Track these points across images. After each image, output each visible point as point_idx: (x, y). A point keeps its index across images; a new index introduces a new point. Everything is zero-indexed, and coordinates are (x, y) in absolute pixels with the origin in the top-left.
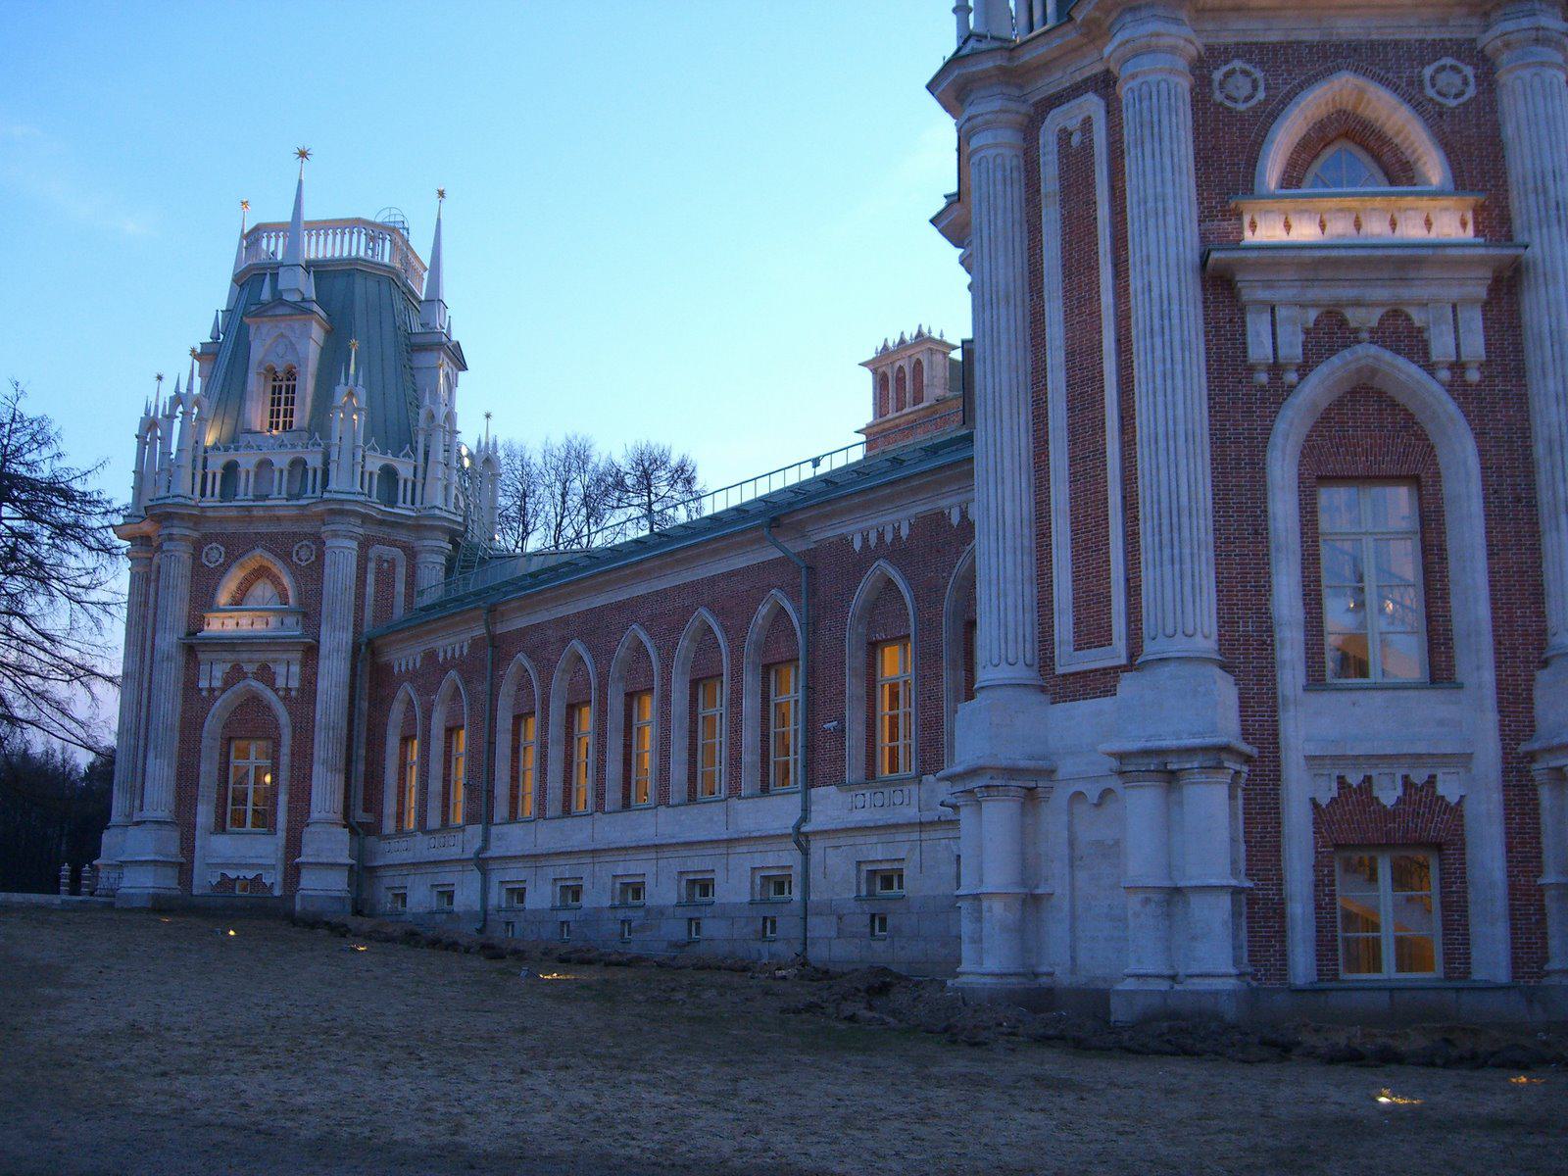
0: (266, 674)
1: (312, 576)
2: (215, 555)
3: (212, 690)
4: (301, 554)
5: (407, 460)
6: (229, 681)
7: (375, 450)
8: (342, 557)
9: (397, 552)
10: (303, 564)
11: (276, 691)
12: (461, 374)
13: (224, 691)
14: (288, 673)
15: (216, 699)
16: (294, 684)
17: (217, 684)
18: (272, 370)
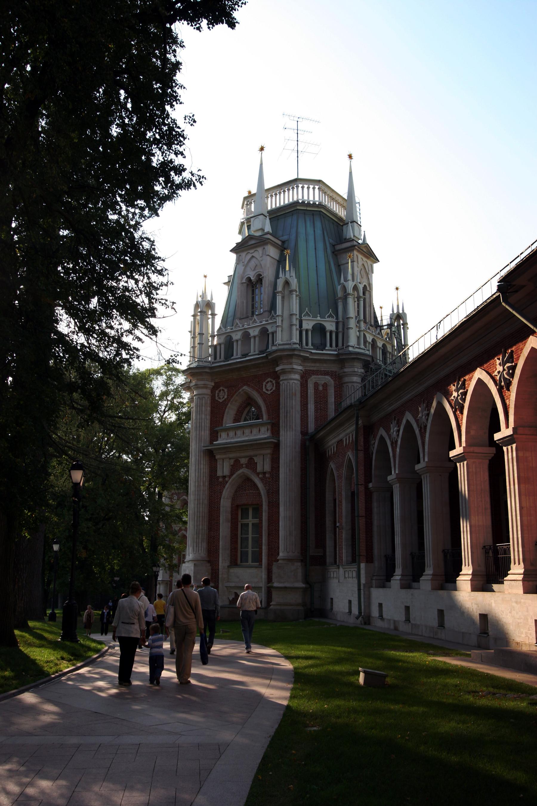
0: (252, 464)
3: (224, 477)
4: (270, 388)
5: (330, 319)
6: (233, 472)
9: (328, 379)
10: (269, 393)
11: (258, 474)
12: (375, 265)
13: (230, 477)
14: (264, 465)
15: (227, 482)
17: (227, 472)
18: (249, 279)
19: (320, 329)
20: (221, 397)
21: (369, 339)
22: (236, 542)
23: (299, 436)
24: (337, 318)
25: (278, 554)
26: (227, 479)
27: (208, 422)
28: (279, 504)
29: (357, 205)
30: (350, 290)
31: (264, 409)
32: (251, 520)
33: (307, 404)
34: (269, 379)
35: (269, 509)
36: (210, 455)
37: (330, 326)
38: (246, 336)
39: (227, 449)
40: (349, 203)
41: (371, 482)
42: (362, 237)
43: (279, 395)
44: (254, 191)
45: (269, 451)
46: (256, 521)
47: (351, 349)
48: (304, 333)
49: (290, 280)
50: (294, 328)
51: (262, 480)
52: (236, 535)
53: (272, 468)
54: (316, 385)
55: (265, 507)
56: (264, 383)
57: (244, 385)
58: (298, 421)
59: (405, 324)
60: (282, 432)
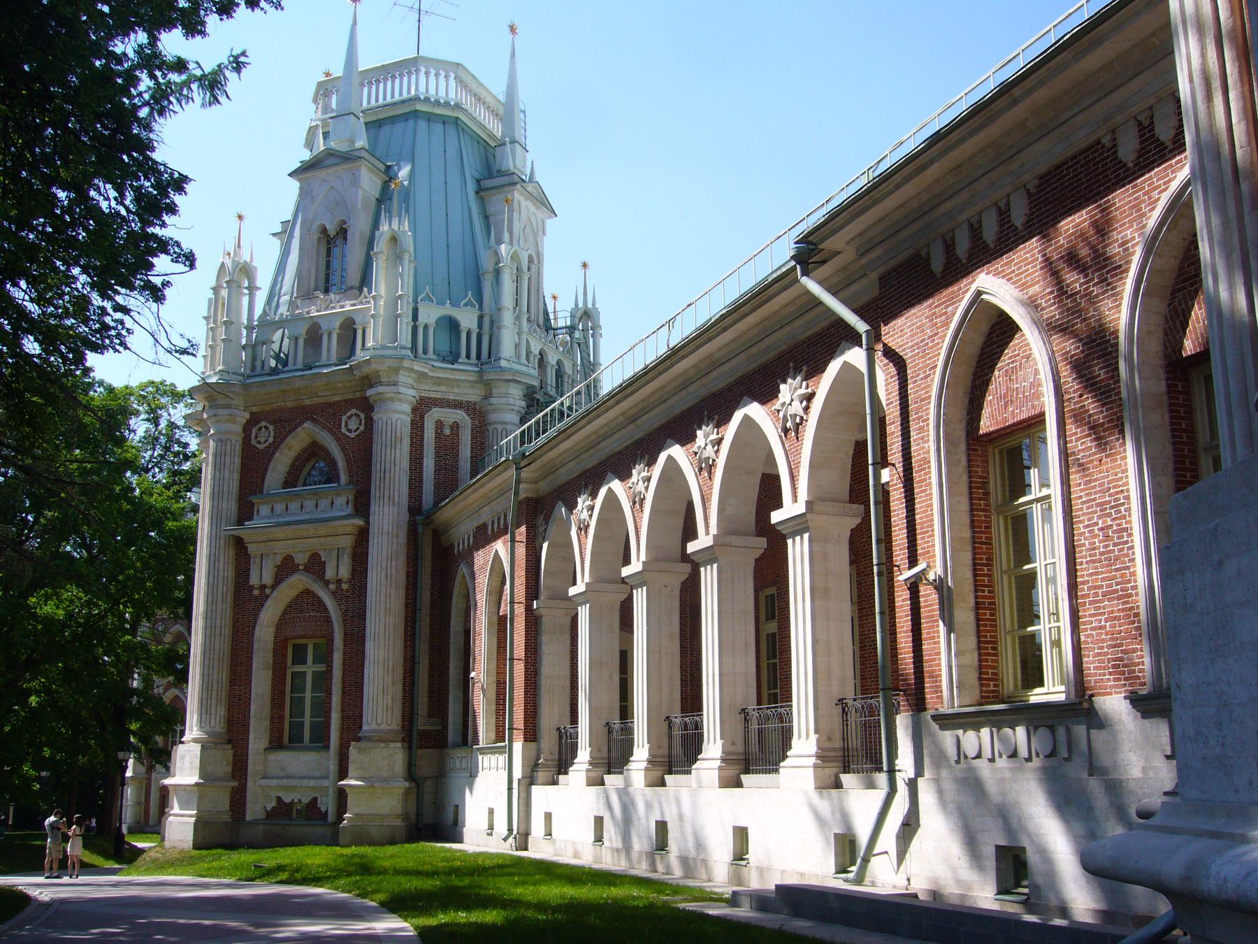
0: (316, 566)
1: (362, 454)
2: (264, 437)
3: (263, 587)
9: (460, 416)
10: (352, 435)
11: (327, 583)
12: (550, 223)
13: (273, 587)
16: (345, 572)
17: (268, 579)
19: (452, 326)
20: (263, 440)
21: (535, 350)
22: (282, 706)
23: (405, 516)
24: (481, 309)
26: (268, 591)
27: (236, 484)
32: (310, 668)
33: (422, 458)
34: (353, 411)
35: (345, 645)
37: (468, 319)
40: (508, 111)
41: (537, 598)
43: (371, 439)
44: (338, 71)
46: (321, 668)
47: (503, 363)
48: (421, 331)
51: (334, 593)
53: (354, 571)
54: (439, 425)
56: (344, 418)
57: (307, 419)
59: (596, 327)
60: (375, 508)
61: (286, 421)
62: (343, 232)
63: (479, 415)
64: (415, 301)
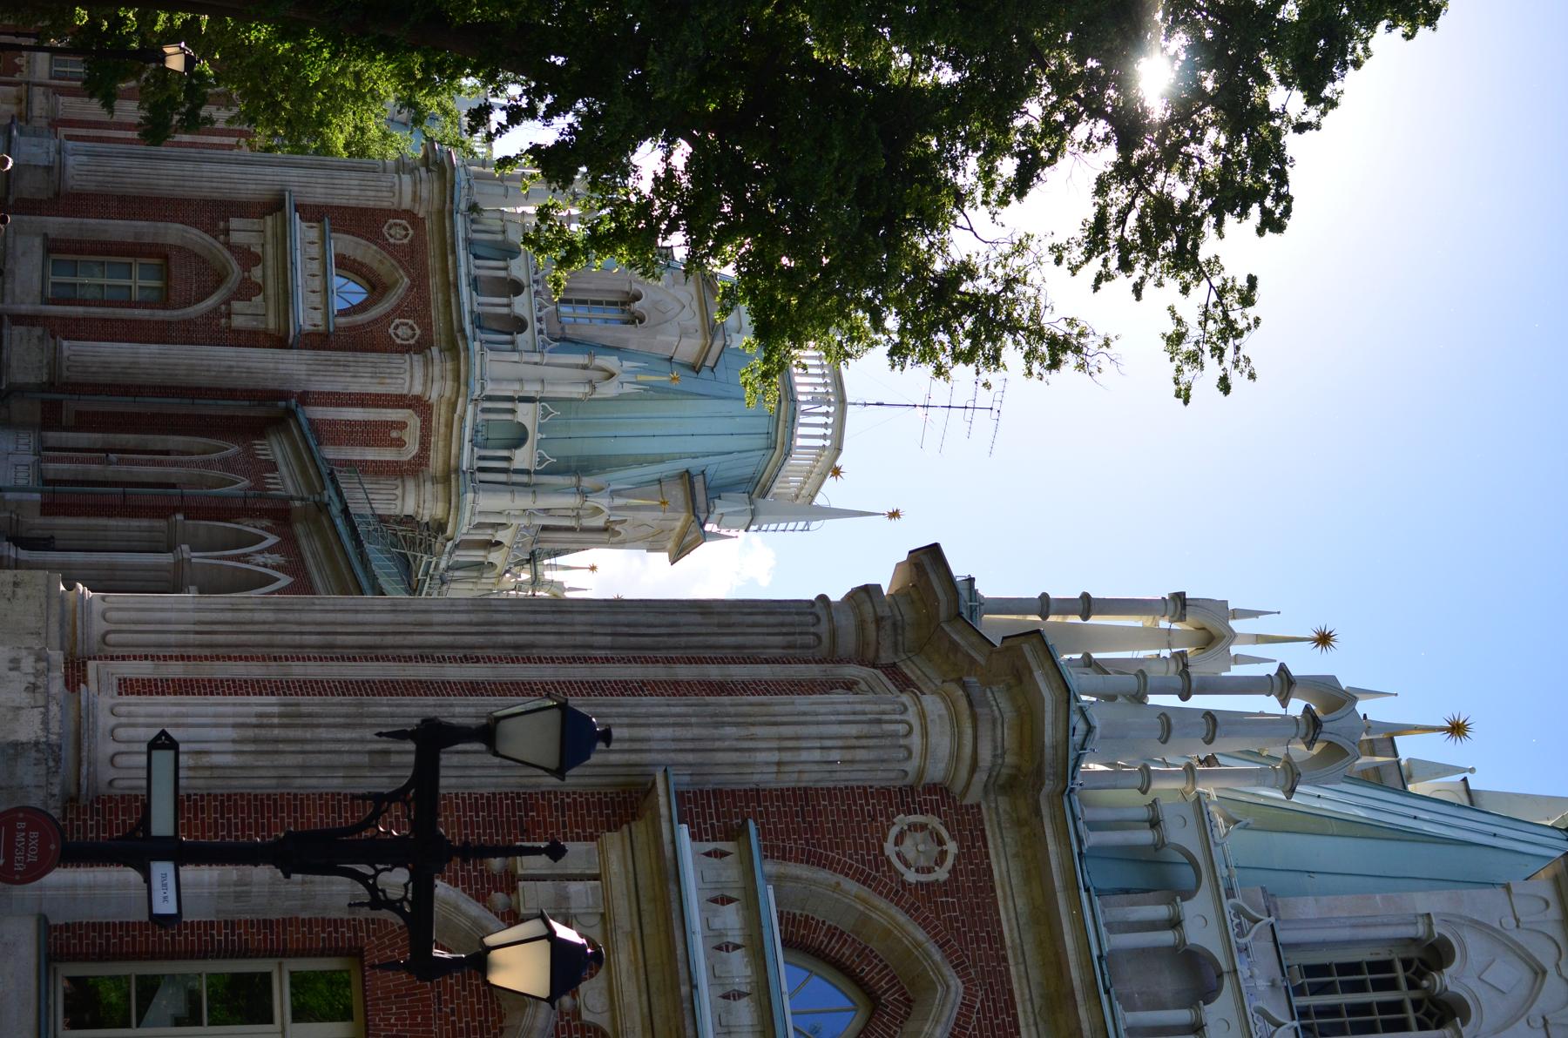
0: (248, 290)
3: (227, 232)
7: (544, 416)
8: (408, 377)
9: (412, 448)
10: (391, 331)
11: (227, 303)
12: (664, 556)
13: (227, 245)
15: (216, 237)
16: (238, 322)
17: (236, 238)
19: (519, 439)
21: (501, 536)
24: (537, 473)
25: (67, 338)
26: (222, 237)
27: (344, 202)
28: (164, 343)
29: (801, 525)
30: (594, 501)
31: (359, 318)
33: (363, 405)
34: (418, 332)
35: (157, 322)
36: (275, 205)
37: (523, 457)
38: (516, 288)
39: (282, 239)
40: (806, 510)
42: (723, 532)
43: (385, 351)
45: (271, 324)
47: (470, 496)
49: (615, 382)
50: (517, 386)
51: (216, 310)
52: (109, 254)
53: (238, 332)
54: (402, 425)
55: (161, 314)
56: (410, 322)
57: (413, 280)
58: (328, 388)
60: (307, 354)
61: (411, 257)
62: (636, 319)
63: (414, 470)
64: (542, 400)
